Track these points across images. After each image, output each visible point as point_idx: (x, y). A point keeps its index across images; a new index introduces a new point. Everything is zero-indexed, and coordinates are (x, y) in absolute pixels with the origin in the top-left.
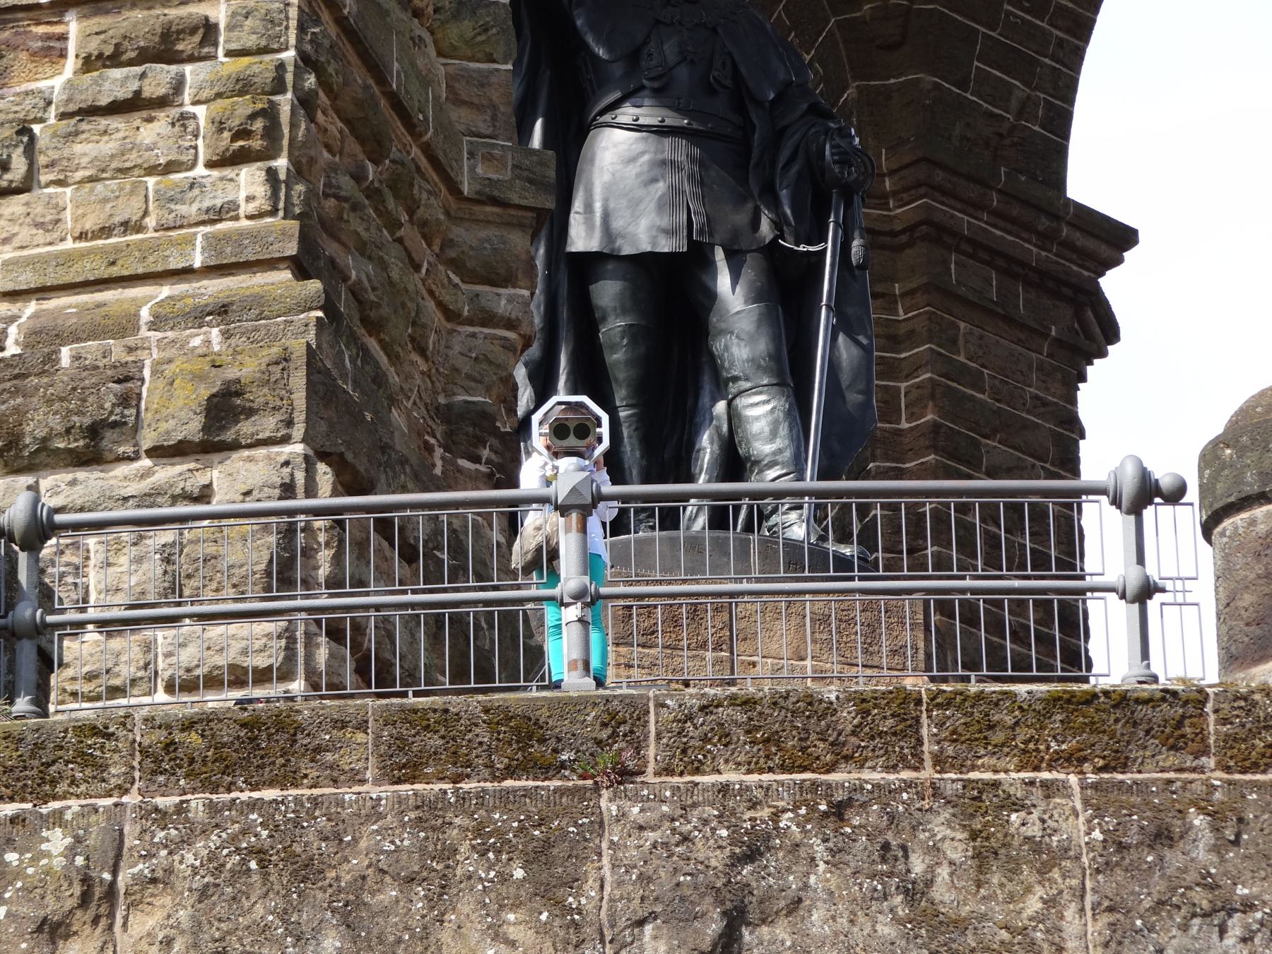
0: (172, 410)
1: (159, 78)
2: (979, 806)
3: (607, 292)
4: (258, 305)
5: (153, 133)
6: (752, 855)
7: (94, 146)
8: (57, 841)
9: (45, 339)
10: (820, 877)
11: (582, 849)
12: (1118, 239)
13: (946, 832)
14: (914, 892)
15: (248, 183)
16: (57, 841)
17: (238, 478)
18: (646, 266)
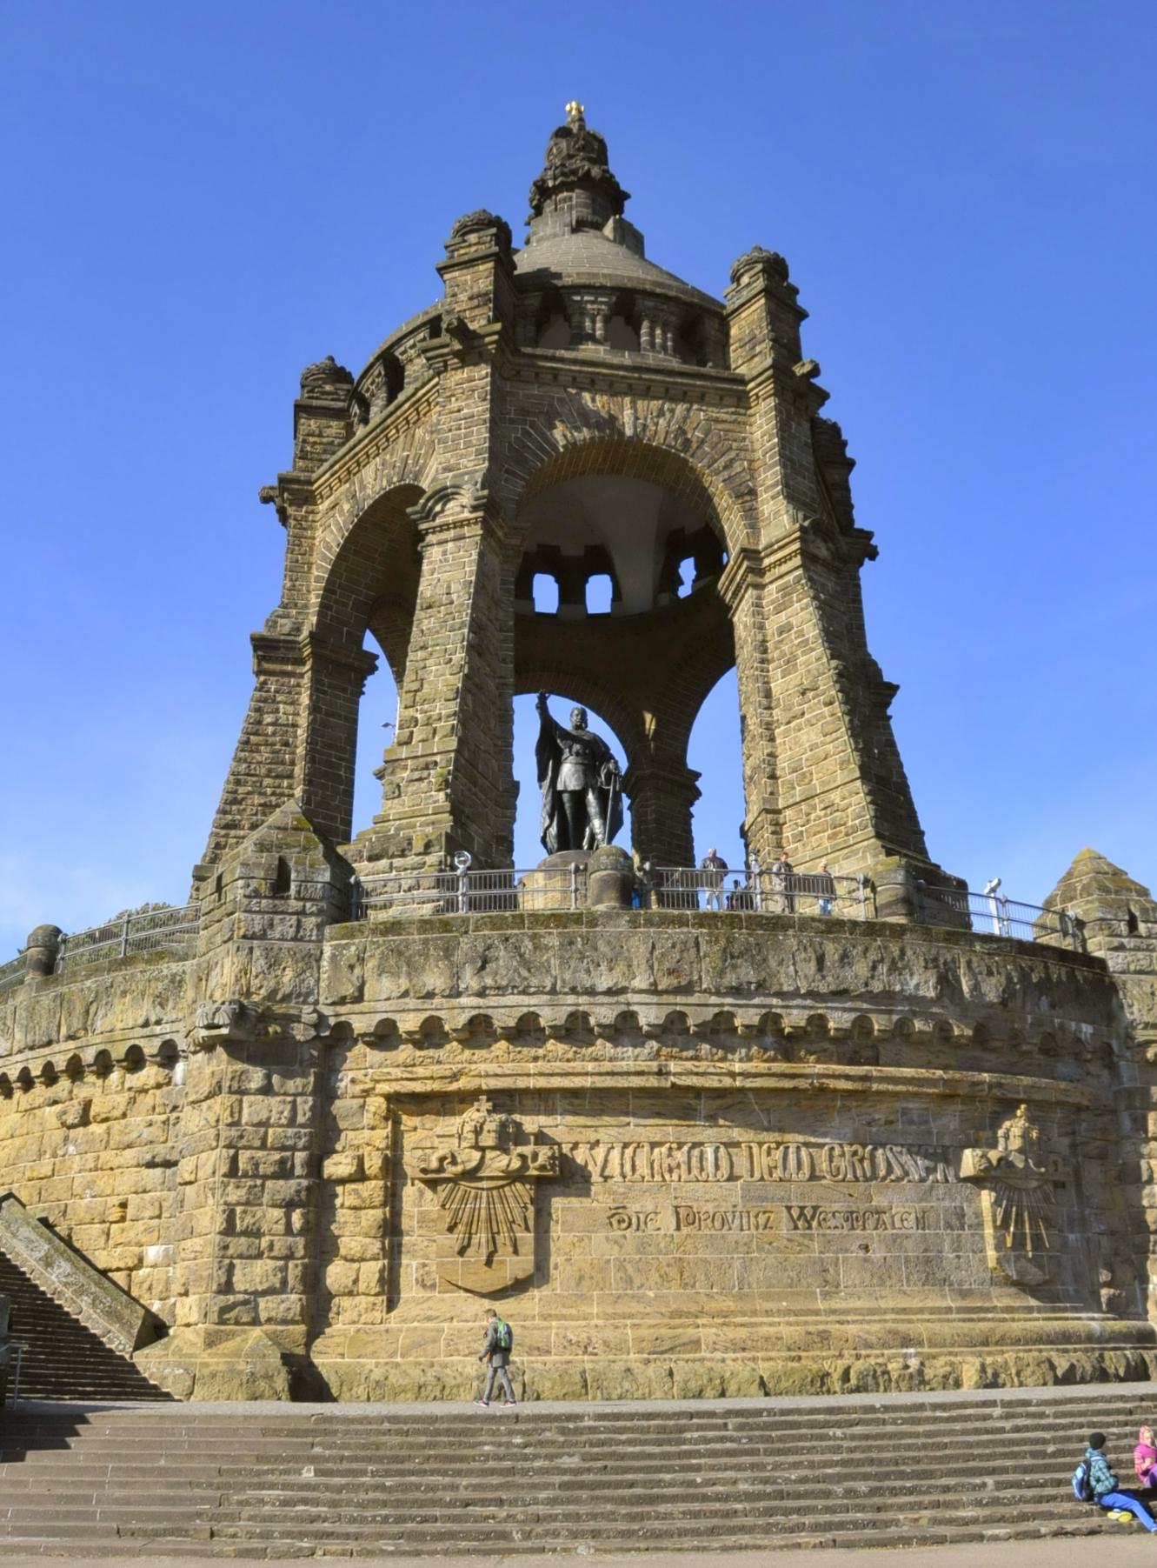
0: (418, 846)
1: (425, 773)
2: (534, 937)
3: (566, 797)
4: (440, 822)
5: (424, 785)
6: (488, 949)
7: (411, 789)
8: (353, 948)
9: (398, 829)
10: (502, 953)
11: (455, 949)
12: (697, 775)
13: (528, 944)
14: (521, 956)
15: (442, 795)
16: (353, 948)
17: (432, 859)
18: (573, 793)
